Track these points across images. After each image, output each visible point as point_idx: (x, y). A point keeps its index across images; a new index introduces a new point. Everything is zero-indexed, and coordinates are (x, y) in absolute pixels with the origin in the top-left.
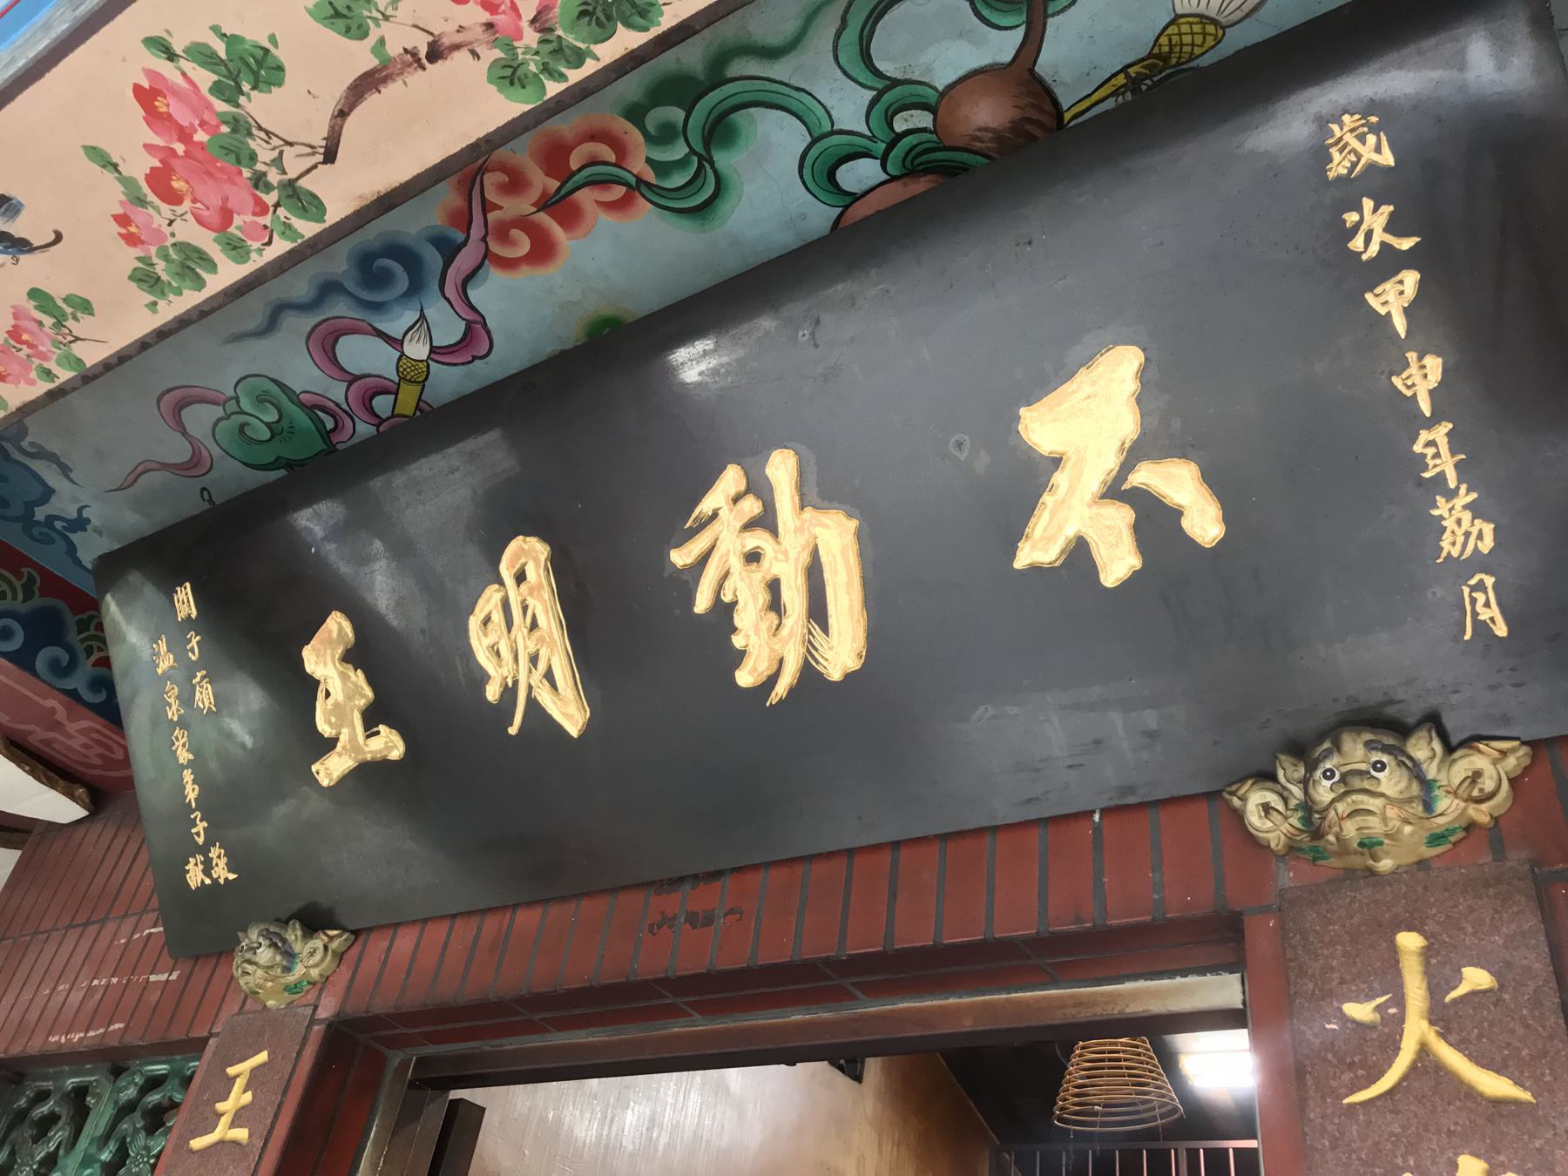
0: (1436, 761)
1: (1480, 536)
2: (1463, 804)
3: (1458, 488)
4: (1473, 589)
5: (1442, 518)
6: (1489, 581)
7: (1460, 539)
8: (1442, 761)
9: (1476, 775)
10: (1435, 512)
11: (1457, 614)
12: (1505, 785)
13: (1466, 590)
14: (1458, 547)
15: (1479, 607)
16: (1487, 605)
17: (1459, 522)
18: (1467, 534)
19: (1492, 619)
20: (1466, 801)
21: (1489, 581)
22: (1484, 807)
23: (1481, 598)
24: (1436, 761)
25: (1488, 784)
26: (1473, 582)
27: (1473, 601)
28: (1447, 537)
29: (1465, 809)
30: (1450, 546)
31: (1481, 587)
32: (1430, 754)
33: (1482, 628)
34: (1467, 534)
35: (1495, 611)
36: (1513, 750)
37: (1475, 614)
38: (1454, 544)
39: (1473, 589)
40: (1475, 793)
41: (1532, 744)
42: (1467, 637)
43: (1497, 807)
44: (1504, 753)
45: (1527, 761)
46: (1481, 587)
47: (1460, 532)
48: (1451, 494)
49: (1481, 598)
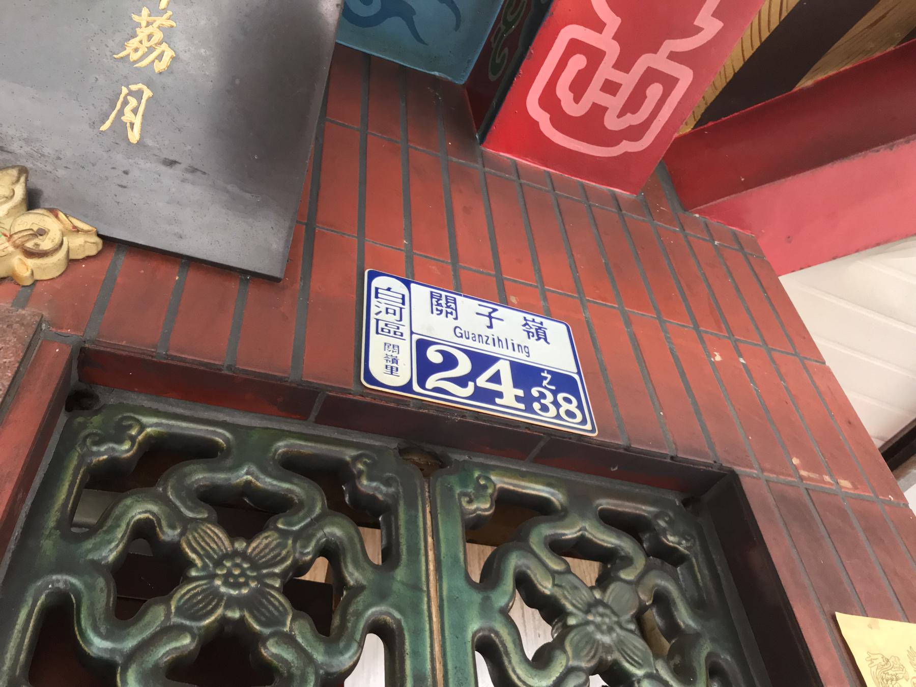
0: (10, 204)
1: (160, 57)
2: (11, 249)
3: (165, 11)
4: (131, 93)
5: (139, 25)
6: (147, 93)
7: (143, 50)
8: (15, 207)
9: (41, 233)
10: (135, 18)
11: (106, 107)
12: (61, 254)
13: (125, 91)
14: (140, 53)
15: (128, 109)
16: (135, 111)
17: (150, 37)
18: (151, 50)
19: (132, 125)
20: (16, 247)
21: (147, 93)
22: (31, 262)
23: (133, 102)
24: (10, 204)
25: (46, 244)
26: (134, 87)
27: (125, 103)
28: (134, 43)
29: (10, 255)
30: (133, 49)
31: (138, 95)
32: (7, 193)
33: (121, 128)
34: (151, 50)
35: (138, 121)
36: (86, 232)
37: (121, 113)
38: (136, 50)
39: (131, 93)
40: (30, 245)
41: (108, 241)
42: (104, 127)
43: (43, 269)
44: (77, 230)
45: (93, 251)
46: (138, 95)
47: (146, 44)
48: (156, 12)
49: (133, 102)
